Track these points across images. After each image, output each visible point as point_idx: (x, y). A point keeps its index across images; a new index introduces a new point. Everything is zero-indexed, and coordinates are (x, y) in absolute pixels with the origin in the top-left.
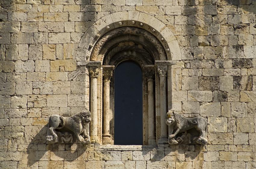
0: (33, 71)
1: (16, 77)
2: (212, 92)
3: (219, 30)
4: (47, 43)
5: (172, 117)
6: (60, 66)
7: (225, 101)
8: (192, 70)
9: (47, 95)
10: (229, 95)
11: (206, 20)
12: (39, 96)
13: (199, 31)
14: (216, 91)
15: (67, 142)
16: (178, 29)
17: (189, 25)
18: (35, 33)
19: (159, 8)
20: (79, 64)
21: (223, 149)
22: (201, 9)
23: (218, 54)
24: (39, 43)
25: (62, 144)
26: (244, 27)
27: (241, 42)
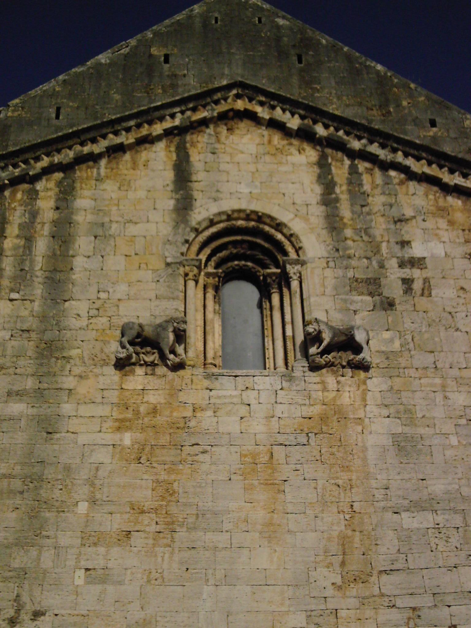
1: (74, 277)
3: (374, 222)
5: (314, 324)
7: (392, 310)
8: (339, 270)
9: (119, 300)
10: (397, 301)
12: (107, 301)
13: (345, 224)
20: (169, 260)
21: (397, 374)
24: (110, 235)
25: (141, 365)
26: (408, 220)
27: (406, 238)
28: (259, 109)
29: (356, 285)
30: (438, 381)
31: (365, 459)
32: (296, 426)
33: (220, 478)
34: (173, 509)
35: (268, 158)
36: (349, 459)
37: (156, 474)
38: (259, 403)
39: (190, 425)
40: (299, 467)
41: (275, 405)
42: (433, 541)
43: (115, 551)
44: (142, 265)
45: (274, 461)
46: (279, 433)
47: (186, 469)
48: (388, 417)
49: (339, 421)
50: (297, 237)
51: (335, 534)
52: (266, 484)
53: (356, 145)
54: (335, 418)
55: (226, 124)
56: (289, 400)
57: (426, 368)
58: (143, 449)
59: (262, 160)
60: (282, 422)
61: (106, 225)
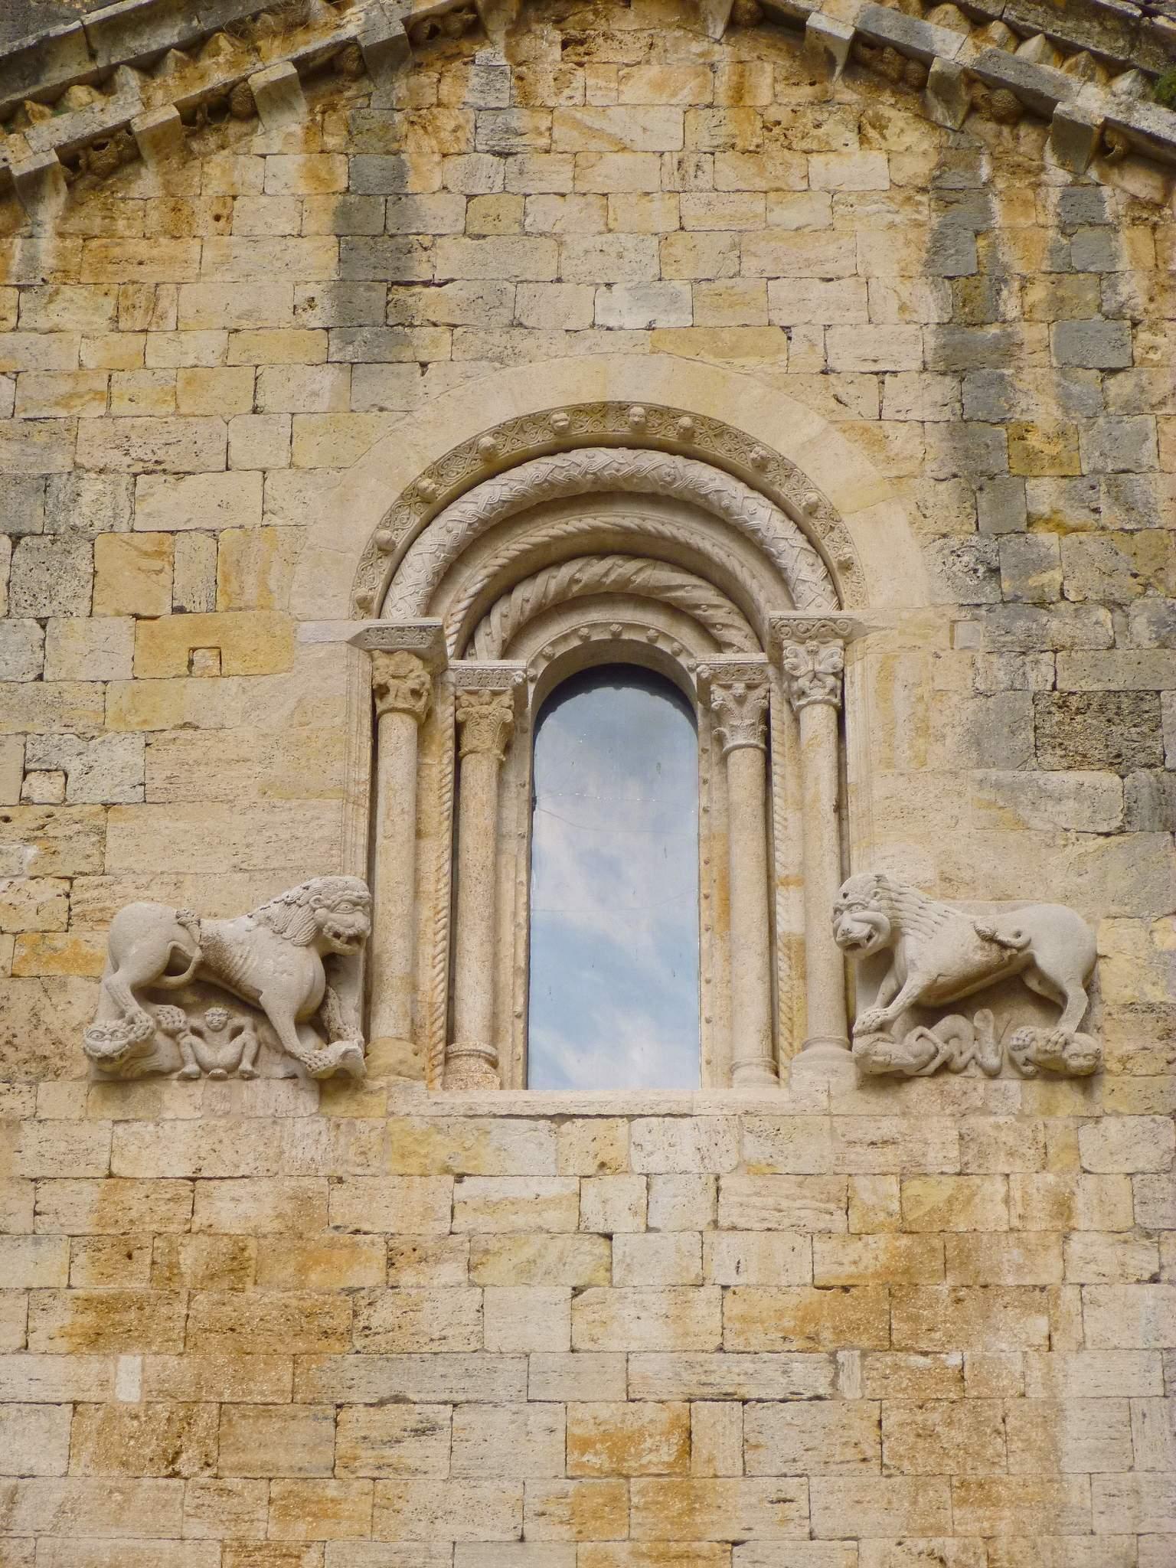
0: (31, 676)
2: (1122, 777)
3: (1151, 444)
4: (125, 527)
6: (194, 650)
9: (107, 806)
11: (1069, 396)
13: (1031, 456)
14: (1144, 774)
15: (218, 1067)
16: (903, 440)
17: (971, 420)
18: (56, 479)
19: (789, 338)
22: (1040, 341)
23: (1147, 571)
24: (74, 528)
25: (188, 1078)
29: (1060, 723)
31: (1051, 1454)
32: (788, 1323)
33: (484, 1534)
35: (728, 171)
36: (989, 1452)
37: (237, 1519)
38: (648, 1229)
39: (374, 1323)
40: (791, 1487)
41: (711, 1236)
44: (197, 656)
45: (699, 1468)
46: (721, 1349)
48: (1155, 1279)
49: (958, 1301)
50: (833, 521)
52: (662, 1557)
54: (944, 1288)
55: (559, 21)
56: (765, 1214)
58: (189, 1420)
59: (704, 181)
60: (735, 1307)
61: (57, 482)
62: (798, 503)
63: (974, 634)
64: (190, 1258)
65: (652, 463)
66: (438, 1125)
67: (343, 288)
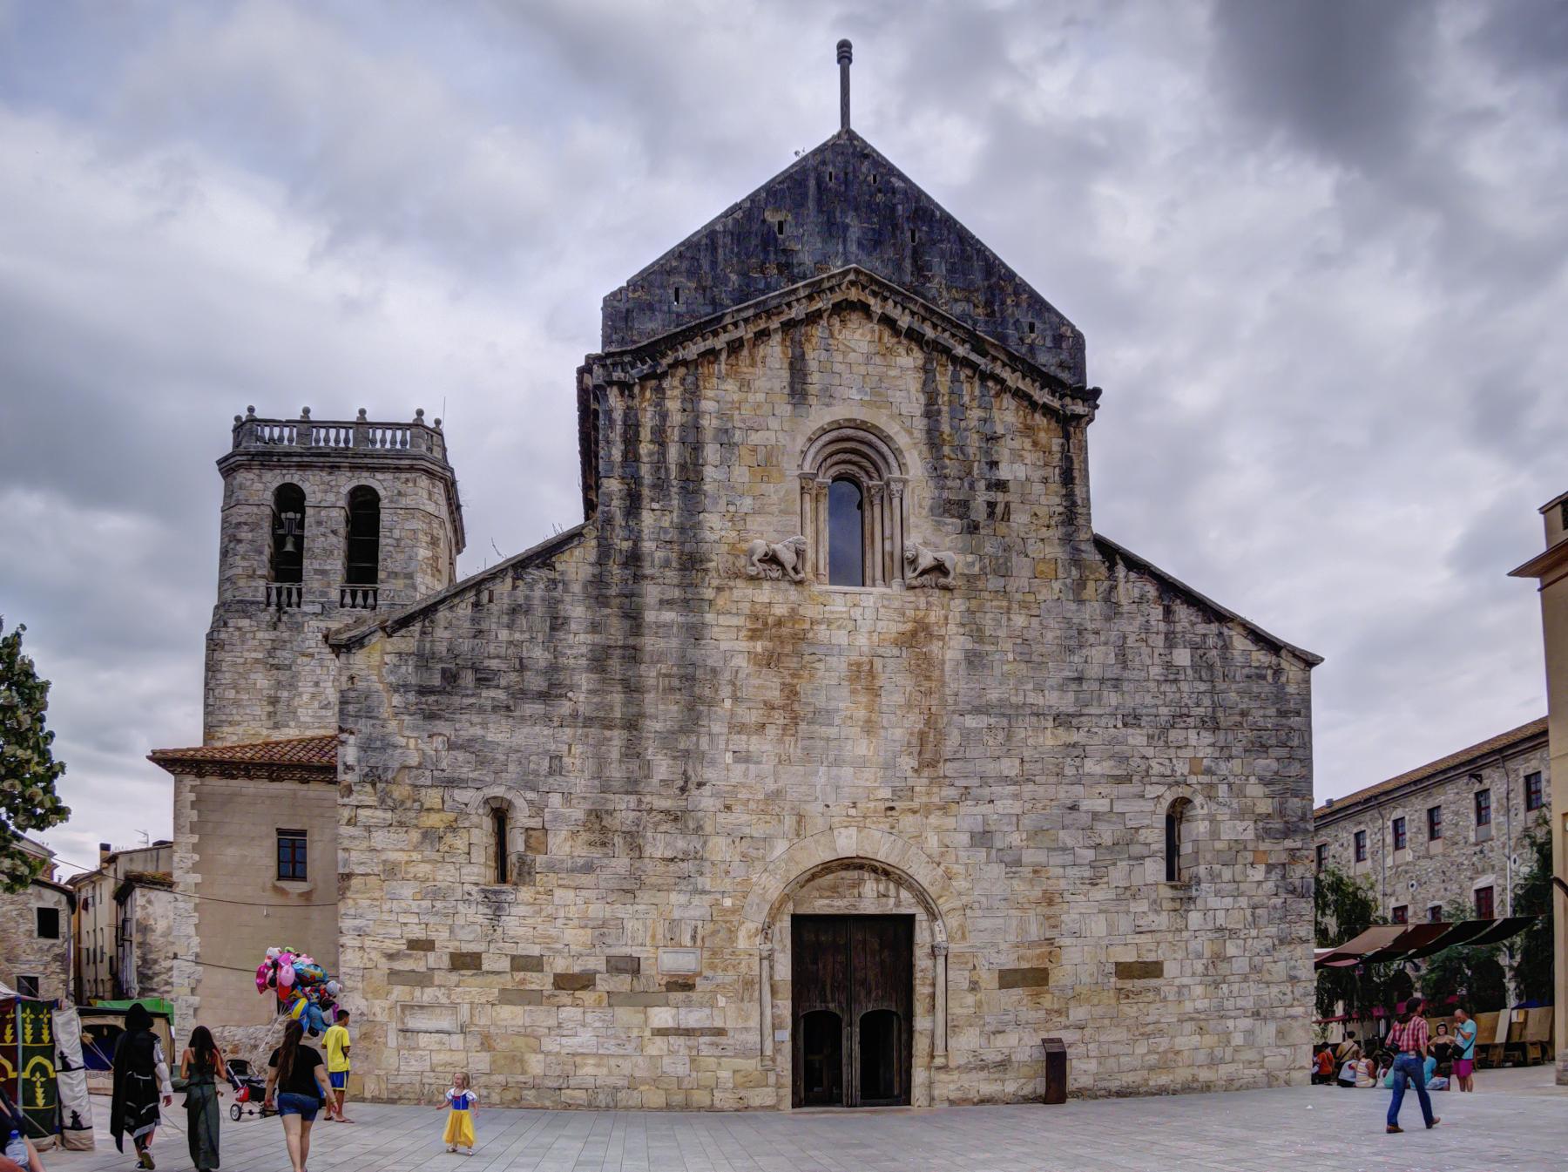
1: (705, 488)
13: (944, 440)
16: (917, 434)
27: (995, 457)
28: (872, 301)
30: (1005, 604)
34: (796, 706)
35: (878, 360)
42: (986, 738)
43: (754, 739)
47: (805, 674)
50: (901, 452)
51: (916, 730)
53: (961, 351)
57: (997, 592)
62: (893, 447)
63: (931, 484)
64: (770, 620)
65: (861, 434)
66: (821, 594)
67: (792, 385)
